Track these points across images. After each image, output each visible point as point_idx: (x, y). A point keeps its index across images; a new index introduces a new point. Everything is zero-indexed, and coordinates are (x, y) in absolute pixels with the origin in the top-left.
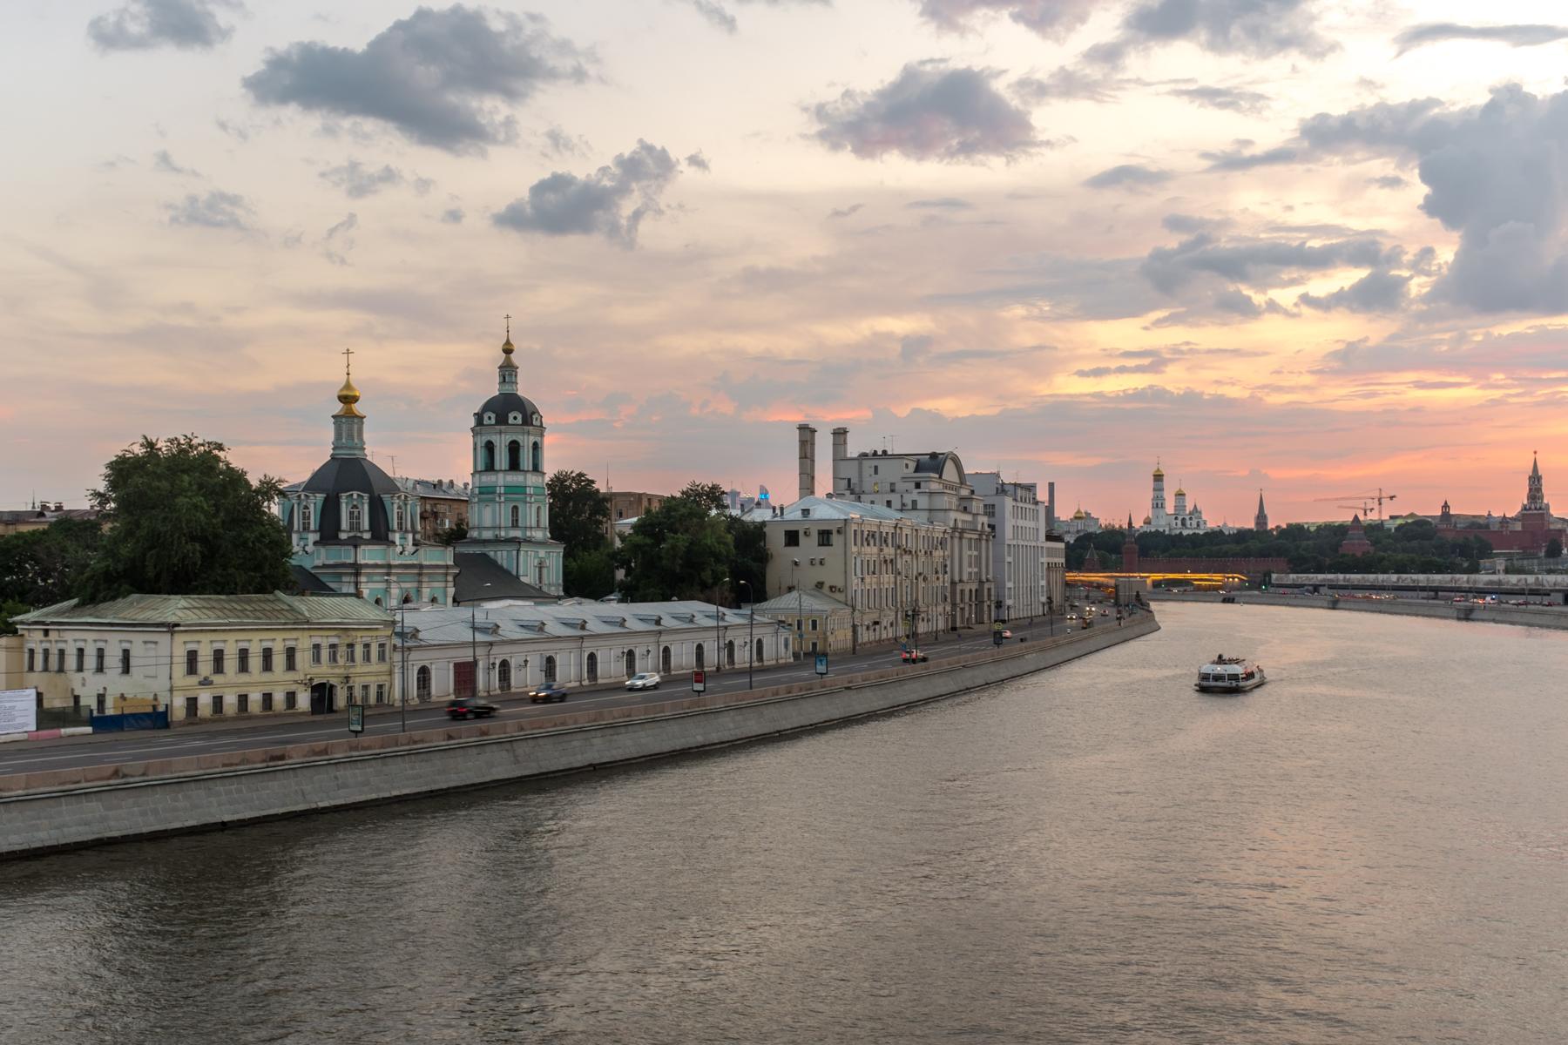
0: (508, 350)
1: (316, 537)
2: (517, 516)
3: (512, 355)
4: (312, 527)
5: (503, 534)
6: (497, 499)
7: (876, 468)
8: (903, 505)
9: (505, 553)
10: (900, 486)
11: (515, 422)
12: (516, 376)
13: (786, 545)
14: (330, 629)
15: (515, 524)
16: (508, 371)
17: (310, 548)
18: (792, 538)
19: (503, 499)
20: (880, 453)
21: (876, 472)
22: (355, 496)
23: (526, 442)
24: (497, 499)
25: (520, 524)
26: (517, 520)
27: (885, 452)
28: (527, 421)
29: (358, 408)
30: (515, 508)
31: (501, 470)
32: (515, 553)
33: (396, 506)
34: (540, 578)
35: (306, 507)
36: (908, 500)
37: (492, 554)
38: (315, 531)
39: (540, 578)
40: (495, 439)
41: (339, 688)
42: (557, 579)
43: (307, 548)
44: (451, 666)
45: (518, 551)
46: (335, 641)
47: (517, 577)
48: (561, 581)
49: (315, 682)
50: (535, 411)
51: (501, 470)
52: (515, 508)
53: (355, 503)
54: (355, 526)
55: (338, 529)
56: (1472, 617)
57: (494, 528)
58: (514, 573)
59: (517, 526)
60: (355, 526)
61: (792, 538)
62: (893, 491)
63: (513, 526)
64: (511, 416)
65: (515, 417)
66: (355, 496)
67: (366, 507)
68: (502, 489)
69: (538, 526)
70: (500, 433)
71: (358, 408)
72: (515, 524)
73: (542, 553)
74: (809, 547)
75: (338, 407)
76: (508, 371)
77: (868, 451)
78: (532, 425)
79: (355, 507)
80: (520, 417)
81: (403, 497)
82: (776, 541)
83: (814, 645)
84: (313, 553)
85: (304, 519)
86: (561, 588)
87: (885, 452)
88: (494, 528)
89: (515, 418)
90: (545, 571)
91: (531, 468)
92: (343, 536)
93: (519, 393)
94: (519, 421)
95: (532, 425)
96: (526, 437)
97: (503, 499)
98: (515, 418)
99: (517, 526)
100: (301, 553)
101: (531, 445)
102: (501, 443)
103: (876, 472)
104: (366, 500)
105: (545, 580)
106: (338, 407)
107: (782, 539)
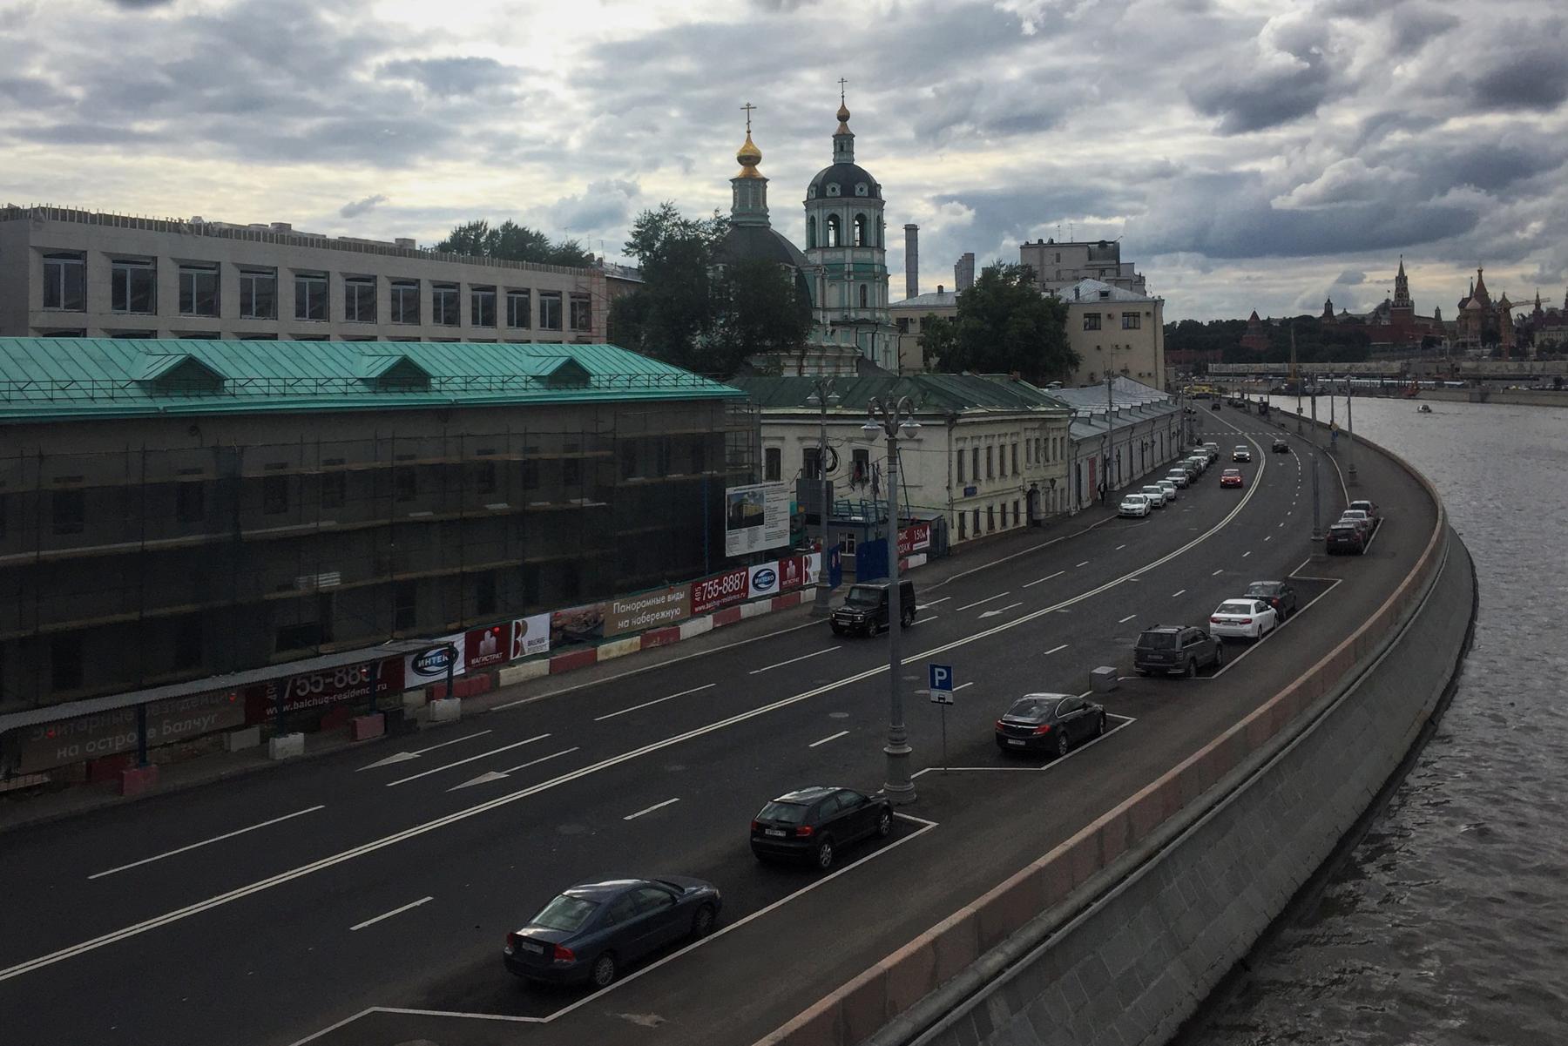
2: (865, 295)
7: (1058, 255)
11: (833, 194)
15: (864, 306)
20: (1045, 241)
24: (846, 277)
25: (868, 305)
29: (762, 169)
31: (848, 246)
45: (873, 334)
51: (848, 246)
56: (1488, 400)
61: (1093, 321)
71: (762, 169)
72: (864, 306)
74: (1113, 332)
75: (738, 170)
78: (854, 196)
94: (838, 193)
95: (854, 196)
96: (872, 210)
98: (834, 190)
102: (819, 215)
103: (1058, 260)
106: (738, 170)
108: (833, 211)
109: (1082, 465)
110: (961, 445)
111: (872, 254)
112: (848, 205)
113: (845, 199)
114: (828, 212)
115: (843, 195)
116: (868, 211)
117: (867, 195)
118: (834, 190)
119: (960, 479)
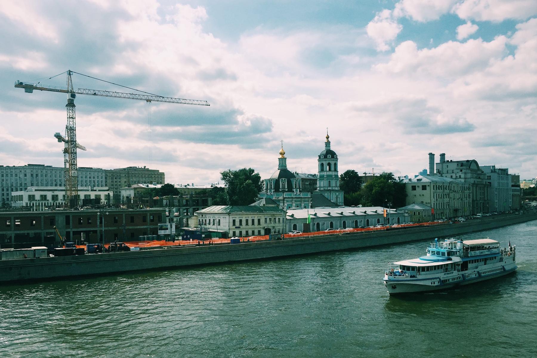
0: (328, 138)
1: (274, 190)
3: (329, 139)
4: (273, 188)
5: (326, 188)
8: (456, 177)
10: (455, 171)
11: (329, 157)
12: (330, 145)
13: (412, 190)
14: (269, 214)
15: (330, 186)
16: (328, 144)
17: (272, 193)
18: (414, 188)
19: (326, 179)
20: (450, 161)
22: (283, 179)
23: (332, 163)
26: (330, 185)
28: (333, 157)
29: (285, 156)
30: (329, 181)
33: (294, 182)
34: (337, 201)
35: (271, 183)
36: (458, 175)
37: (323, 194)
38: (273, 189)
39: (337, 201)
40: (324, 162)
41: (272, 230)
42: (342, 201)
43: (271, 194)
44: (303, 224)
45: (330, 193)
46: (271, 217)
47: (330, 200)
48: (343, 202)
49: (266, 228)
50: (335, 154)
52: (329, 181)
53: (283, 181)
54: (284, 187)
55: (279, 188)
57: (323, 187)
58: (329, 199)
59: (330, 186)
60: (284, 187)
62: (453, 173)
63: (329, 186)
64: (328, 156)
65: (329, 156)
66: (283, 179)
67: (286, 182)
68: (326, 176)
69: (336, 186)
70: (325, 160)
72: (330, 186)
73: (337, 194)
74: (419, 190)
76: (328, 144)
79: (283, 182)
80: (330, 156)
81: (296, 179)
82: (409, 188)
83: (419, 219)
84: (273, 195)
85: (271, 186)
86: (343, 203)
88: (323, 187)
90: (338, 199)
91: (334, 170)
92: (281, 190)
93: (331, 149)
97: (326, 179)
98: (329, 156)
99: (330, 186)
100: (270, 195)
101: (334, 164)
102: (325, 163)
103: (447, 167)
104: (286, 181)
105: (338, 202)
108: (329, 162)
112: (333, 160)
113: (332, 159)
114: (328, 162)
115: (332, 158)
118: (329, 156)
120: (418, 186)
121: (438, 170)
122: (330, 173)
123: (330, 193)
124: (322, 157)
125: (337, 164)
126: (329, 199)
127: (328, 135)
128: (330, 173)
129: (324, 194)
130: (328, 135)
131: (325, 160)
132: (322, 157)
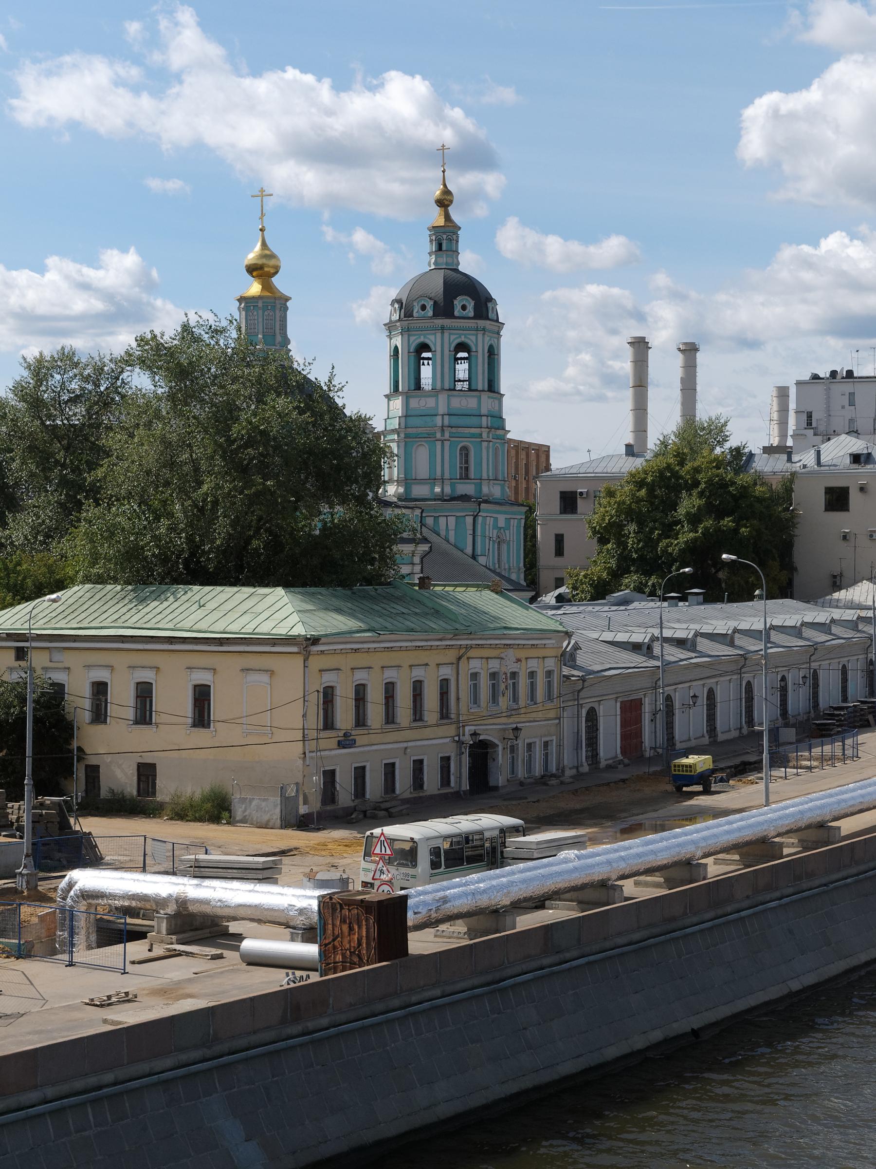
6: (438, 435)
9: (452, 521)
13: (826, 510)
19: (447, 435)
21: (852, 403)
26: (467, 469)
27: (850, 374)
32: (469, 520)
57: (432, 480)
59: (467, 477)
65: (463, 304)
70: (443, 329)
77: (824, 372)
87: (850, 374)
88: (432, 480)
89: (464, 308)
90: (504, 547)
97: (447, 435)
99: (467, 477)
107: (820, 499)
109: (601, 711)
110: (329, 679)
111: (479, 398)
116: (473, 338)
117: (472, 314)
119: (328, 724)
120: (862, 489)
121: (804, 417)
122: (471, 403)
123: (475, 517)
124: (423, 308)
125: (498, 355)
126: (469, 550)
127: (445, 185)
128: (471, 403)
129: (436, 518)
130: (445, 185)
131: (443, 329)
132: (423, 308)
